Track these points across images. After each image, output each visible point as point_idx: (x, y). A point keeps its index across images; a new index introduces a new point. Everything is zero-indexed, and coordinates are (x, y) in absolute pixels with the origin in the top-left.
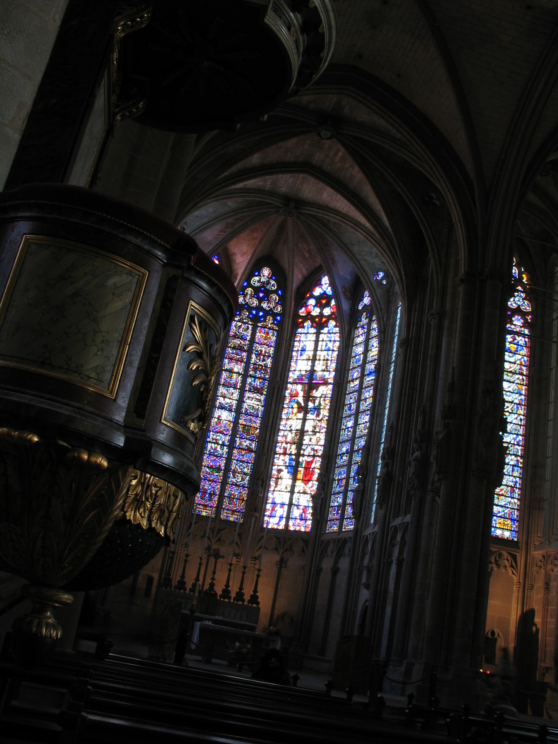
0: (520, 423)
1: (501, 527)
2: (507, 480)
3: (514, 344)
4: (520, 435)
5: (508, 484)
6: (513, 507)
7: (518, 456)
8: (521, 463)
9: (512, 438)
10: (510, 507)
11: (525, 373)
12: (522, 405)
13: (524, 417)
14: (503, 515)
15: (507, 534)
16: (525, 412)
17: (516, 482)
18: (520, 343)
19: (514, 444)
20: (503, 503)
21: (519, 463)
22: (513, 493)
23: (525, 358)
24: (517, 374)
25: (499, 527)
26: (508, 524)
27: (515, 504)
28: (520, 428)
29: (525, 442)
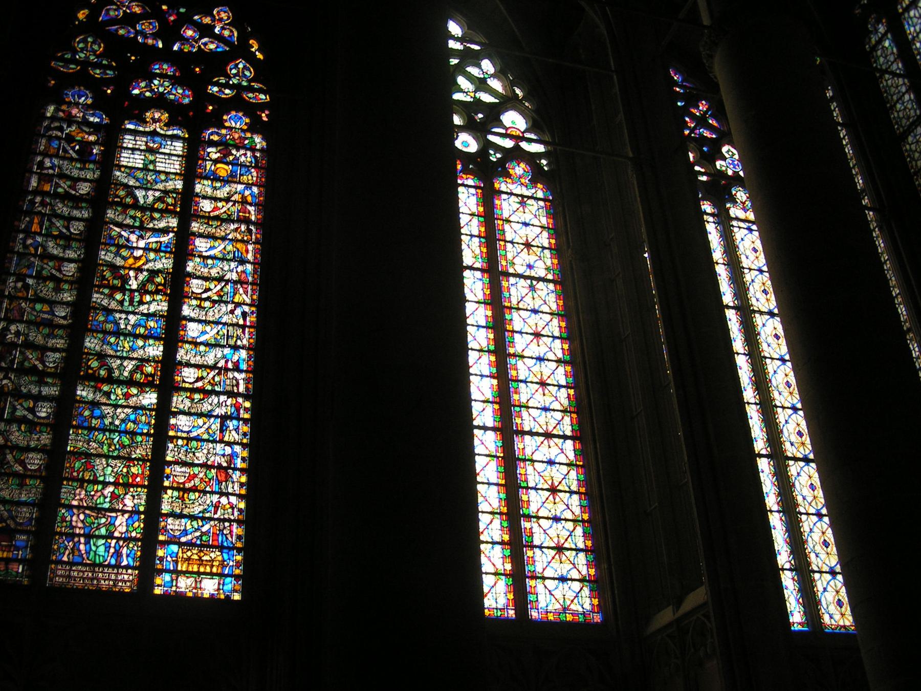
0: (241, 322)
1: (190, 569)
2: (209, 453)
3: (227, 164)
4: (243, 347)
5: (209, 463)
6: (226, 516)
7: (239, 394)
8: (246, 410)
9: (219, 355)
10: (216, 516)
11: (253, 218)
12: (247, 283)
13: (253, 309)
14: (197, 538)
15: (209, 587)
16: (255, 297)
17: (232, 456)
18: (243, 159)
19: (227, 370)
20: (197, 510)
21: (242, 411)
22: (226, 481)
23: (255, 190)
24: (233, 222)
25: (184, 569)
26: (213, 561)
27: (233, 509)
28: (244, 332)
29: (255, 362)
